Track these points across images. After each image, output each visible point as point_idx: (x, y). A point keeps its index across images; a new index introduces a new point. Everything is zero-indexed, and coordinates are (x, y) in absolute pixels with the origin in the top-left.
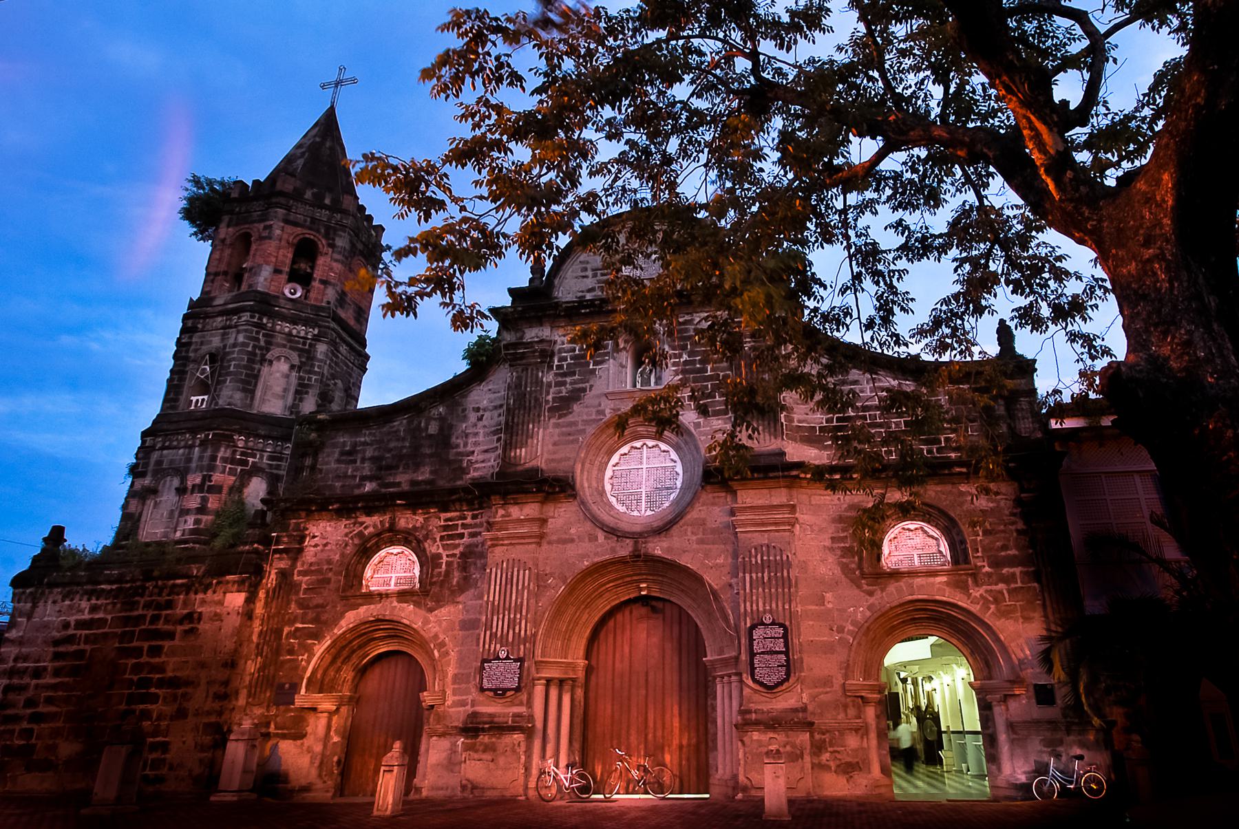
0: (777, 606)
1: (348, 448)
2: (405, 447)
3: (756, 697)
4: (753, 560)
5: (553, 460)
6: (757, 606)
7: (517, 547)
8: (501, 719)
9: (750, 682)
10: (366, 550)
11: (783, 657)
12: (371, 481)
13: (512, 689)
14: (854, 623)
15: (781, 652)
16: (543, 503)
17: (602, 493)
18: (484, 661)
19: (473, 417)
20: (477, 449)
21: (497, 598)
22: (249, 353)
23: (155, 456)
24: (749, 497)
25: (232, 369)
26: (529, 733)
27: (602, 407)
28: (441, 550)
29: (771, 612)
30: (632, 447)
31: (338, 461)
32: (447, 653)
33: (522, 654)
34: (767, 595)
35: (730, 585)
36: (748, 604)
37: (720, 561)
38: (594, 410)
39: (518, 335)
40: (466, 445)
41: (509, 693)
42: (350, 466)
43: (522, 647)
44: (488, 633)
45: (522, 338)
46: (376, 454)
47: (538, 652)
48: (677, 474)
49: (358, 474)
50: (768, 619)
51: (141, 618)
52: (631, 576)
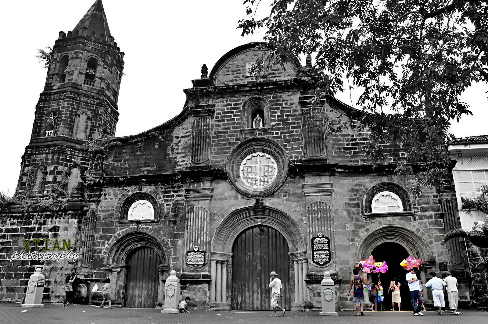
4: (313, 209)
6: (315, 229)
9: (312, 262)
10: (129, 202)
11: (327, 252)
16: (212, 181)
19: (175, 141)
20: (178, 156)
22: (70, 111)
23: (32, 158)
25: (63, 118)
28: (164, 202)
29: (321, 232)
30: (252, 156)
33: (205, 250)
34: (320, 224)
36: (311, 228)
37: (297, 209)
41: (200, 266)
42: (119, 163)
43: (205, 246)
48: (275, 169)
51: (33, 229)
52: (254, 216)
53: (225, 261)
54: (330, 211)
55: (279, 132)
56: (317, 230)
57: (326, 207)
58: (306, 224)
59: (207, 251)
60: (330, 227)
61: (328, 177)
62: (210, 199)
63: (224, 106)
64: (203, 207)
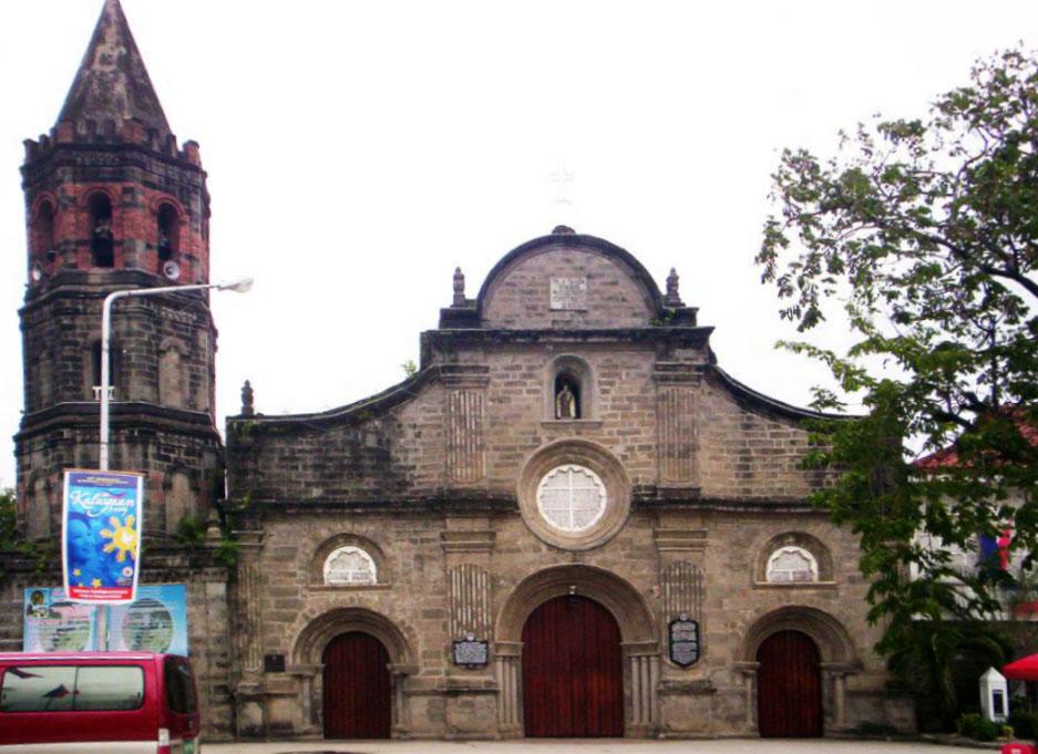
1: (287, 454)
2: (345, 457)
3: (672, 672)
5: (495, 481)
9: (669, 661)
10: (325, 548)
11: (694, 645)
12: (317, 487)
14: (744, 621)
17: (536, 510)
18: (455, 642)
19: (410, 433)
24: (670, 524)
26: (495, 693)
27: (538, 435)
29: (686, 612)
31: (278, 466)
32: (414, 636)
33: (486, 638)
35: (652, 591)
37: (644, 572)
38: (531, 437)
39: (452, 356)
40: (406, 459)
44: (455, 622)
45: (456, 360)
46: (317, 462)
47: (496, 637)
49: (302, 480)
50: (684, 617)
54: (701, 577)
55: (615, 430)
58: (658, 597)
61: (699, 519)
63: (506, 368)
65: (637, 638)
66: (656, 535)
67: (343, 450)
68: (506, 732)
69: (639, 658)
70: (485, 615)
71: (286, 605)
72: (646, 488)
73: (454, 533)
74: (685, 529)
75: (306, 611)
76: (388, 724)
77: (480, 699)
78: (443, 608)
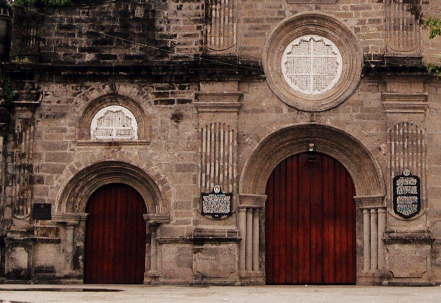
0: (413, 164)
1: (65, 23)
2: (116, 26)
3: (397, 223)
4: (397, 132)
5: (245, 49)
6: (399, 164)
7: (221, 113)
8: (220, 234)
9: (393, 213)
11: (416, 198)
13: (226, 214)
15: (414, 195)
18: (203, 194)
21: (208, 150)
24: (396, 88)
26: (238, 241)
27: (282, 10)
29: (408, 168)
30: (302, 40)
31: (57, 33)
33: (230, 191)
34: (406, 157)
36: (393, 162)
37: (373, 131)
38: (276, 11)
40: (168, 29)
42: (70, 39)
43: (230, 186)
44: (204, 175)
47: (241, 190)
49: (77, 45)
52: (304, 138)
53: (257, 208)
54: (422, 137)
56: (402, 166)
57: (417, 131)
58: (385, 155)
59: (234, 193)
60: (421, 161)
61: (422, 85)
62: (237, 110)
64: (227, 123)
65: (369, 192)
66: (383, 98)
67: (114, 19)
68: (245, 278)
69: (369, 210)
70: (230, 169)
71: (56, 158)
72: (376, 56)
73: (206, 95)
74: (408, 93)
75: (73, 163)
76: (143, 270)
77: (223, 246)
78: (192, 162)
